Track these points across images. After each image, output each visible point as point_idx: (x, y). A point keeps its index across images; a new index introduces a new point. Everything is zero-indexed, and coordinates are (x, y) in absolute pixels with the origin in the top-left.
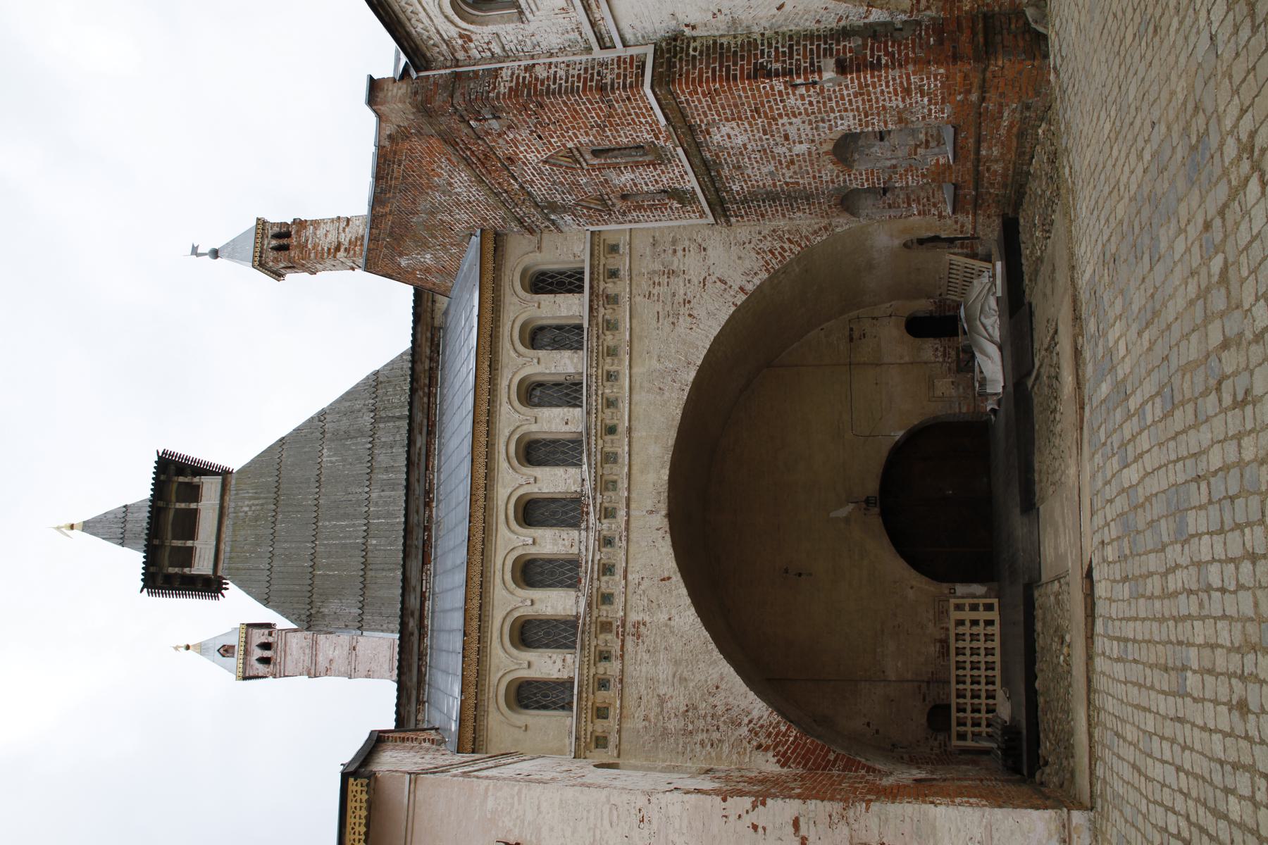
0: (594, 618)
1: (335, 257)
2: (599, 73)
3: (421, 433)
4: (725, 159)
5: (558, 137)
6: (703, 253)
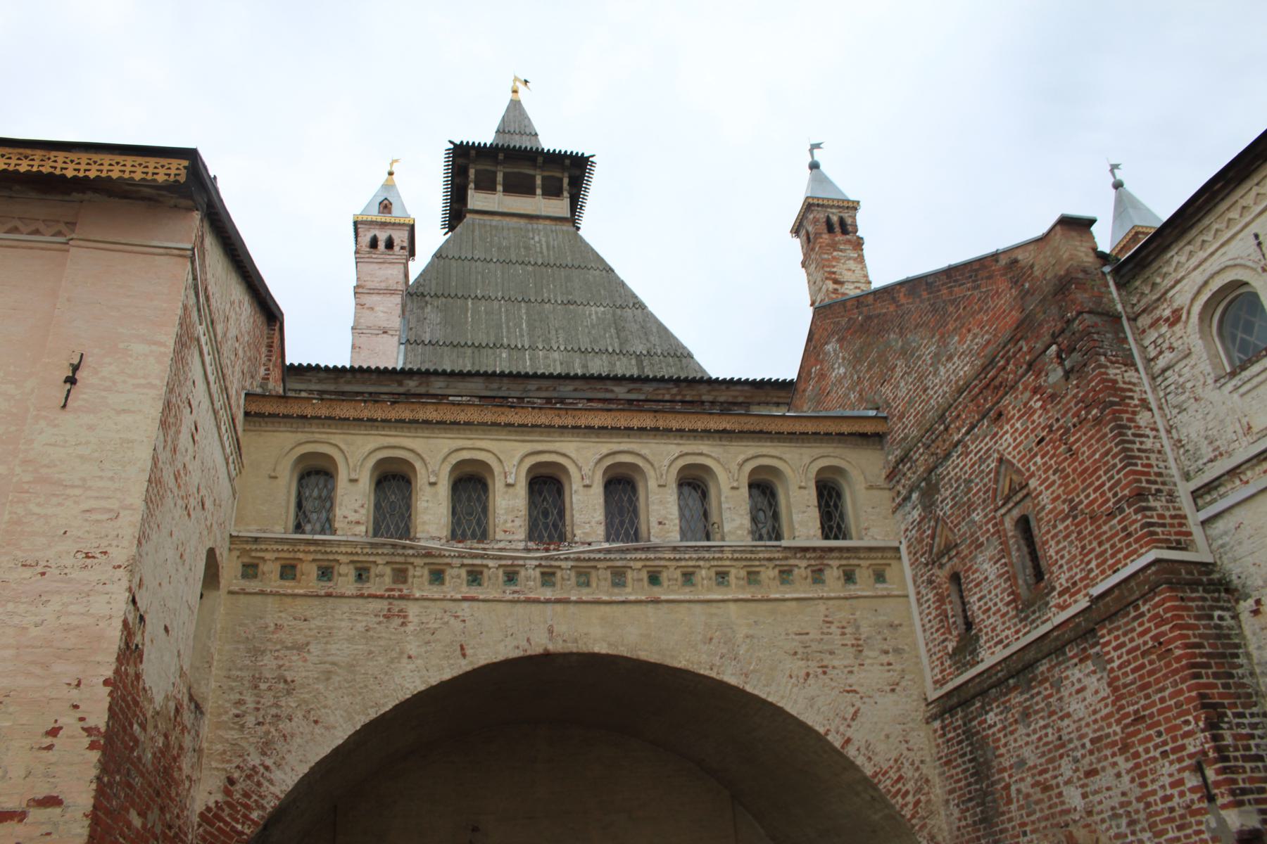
0: (412, 560)
1: (827, 278)
2: (1158, 491)
3: (629, 391)
4: (1039, 693)
5: (1045, 464)
6: (888, 688)
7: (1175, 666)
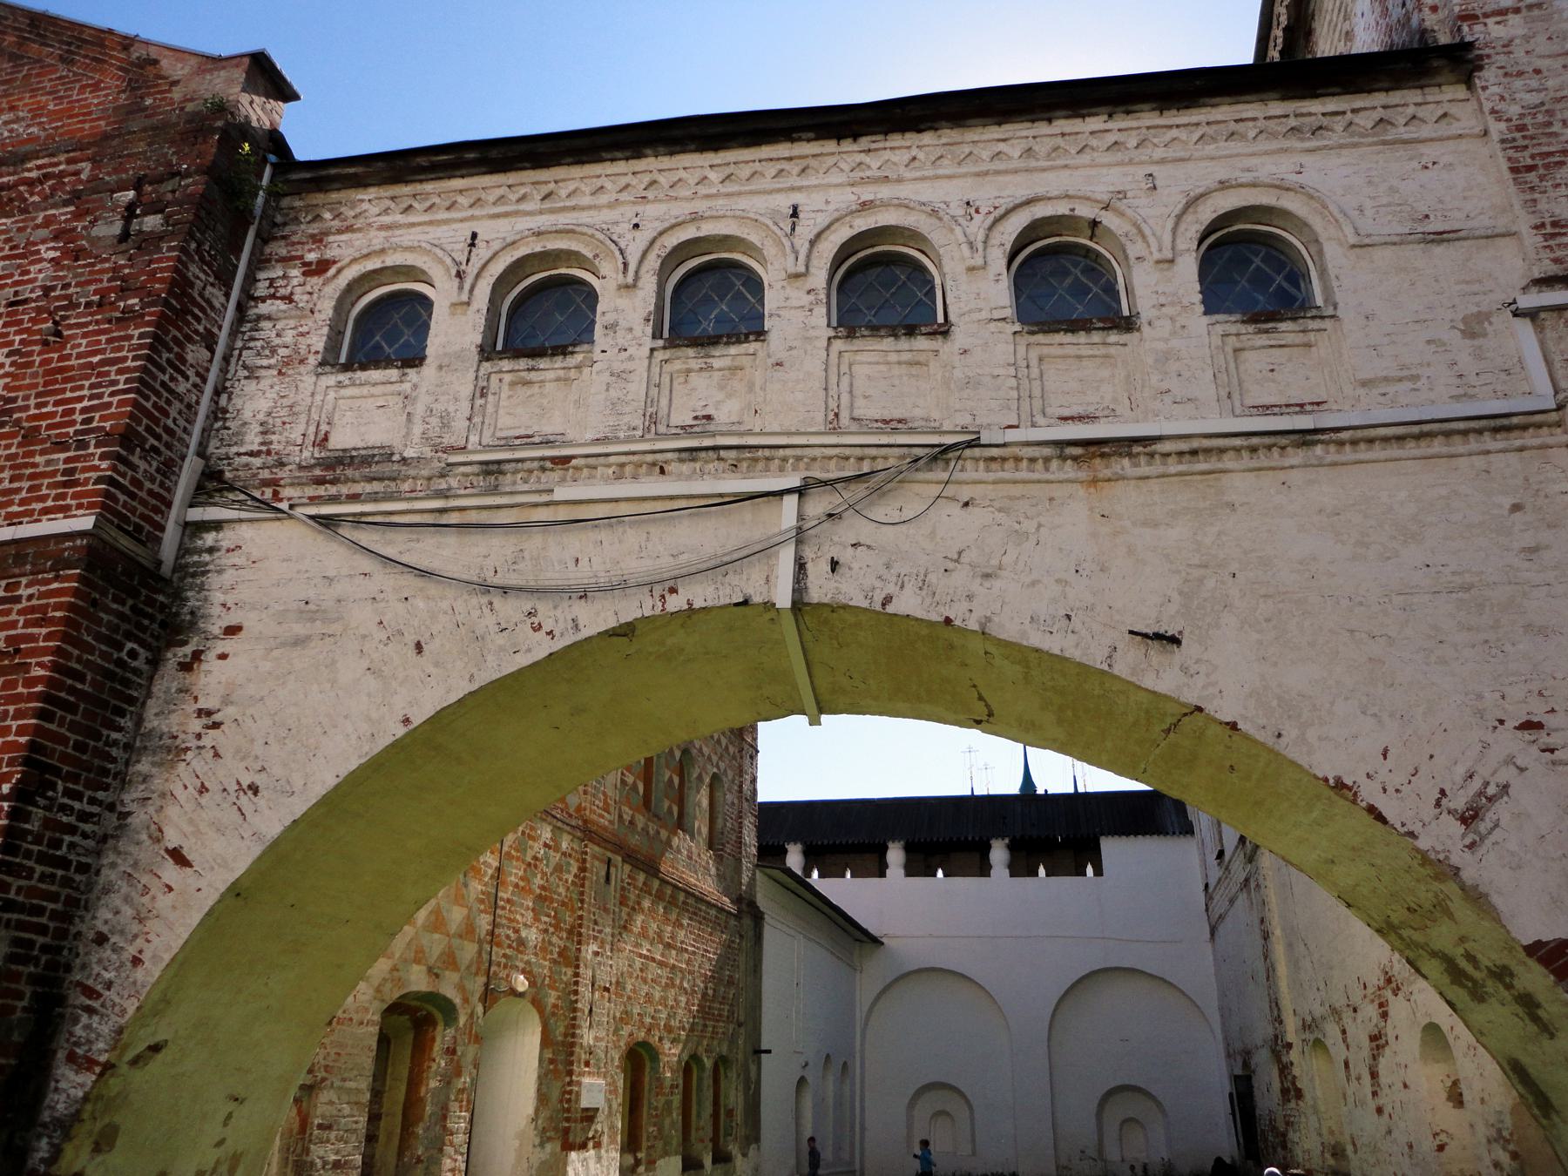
2: (153, 449)
7: (20, 689)
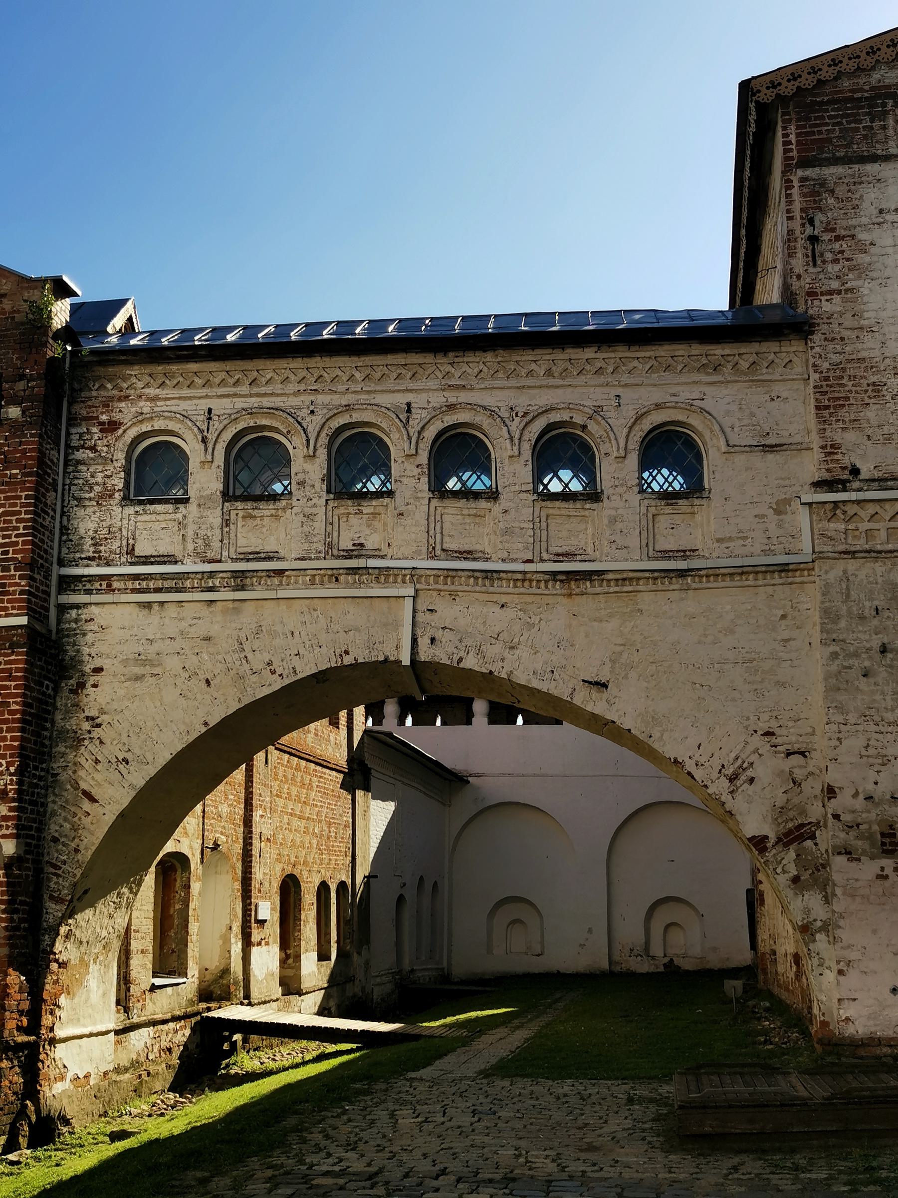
7: (7, 716)
